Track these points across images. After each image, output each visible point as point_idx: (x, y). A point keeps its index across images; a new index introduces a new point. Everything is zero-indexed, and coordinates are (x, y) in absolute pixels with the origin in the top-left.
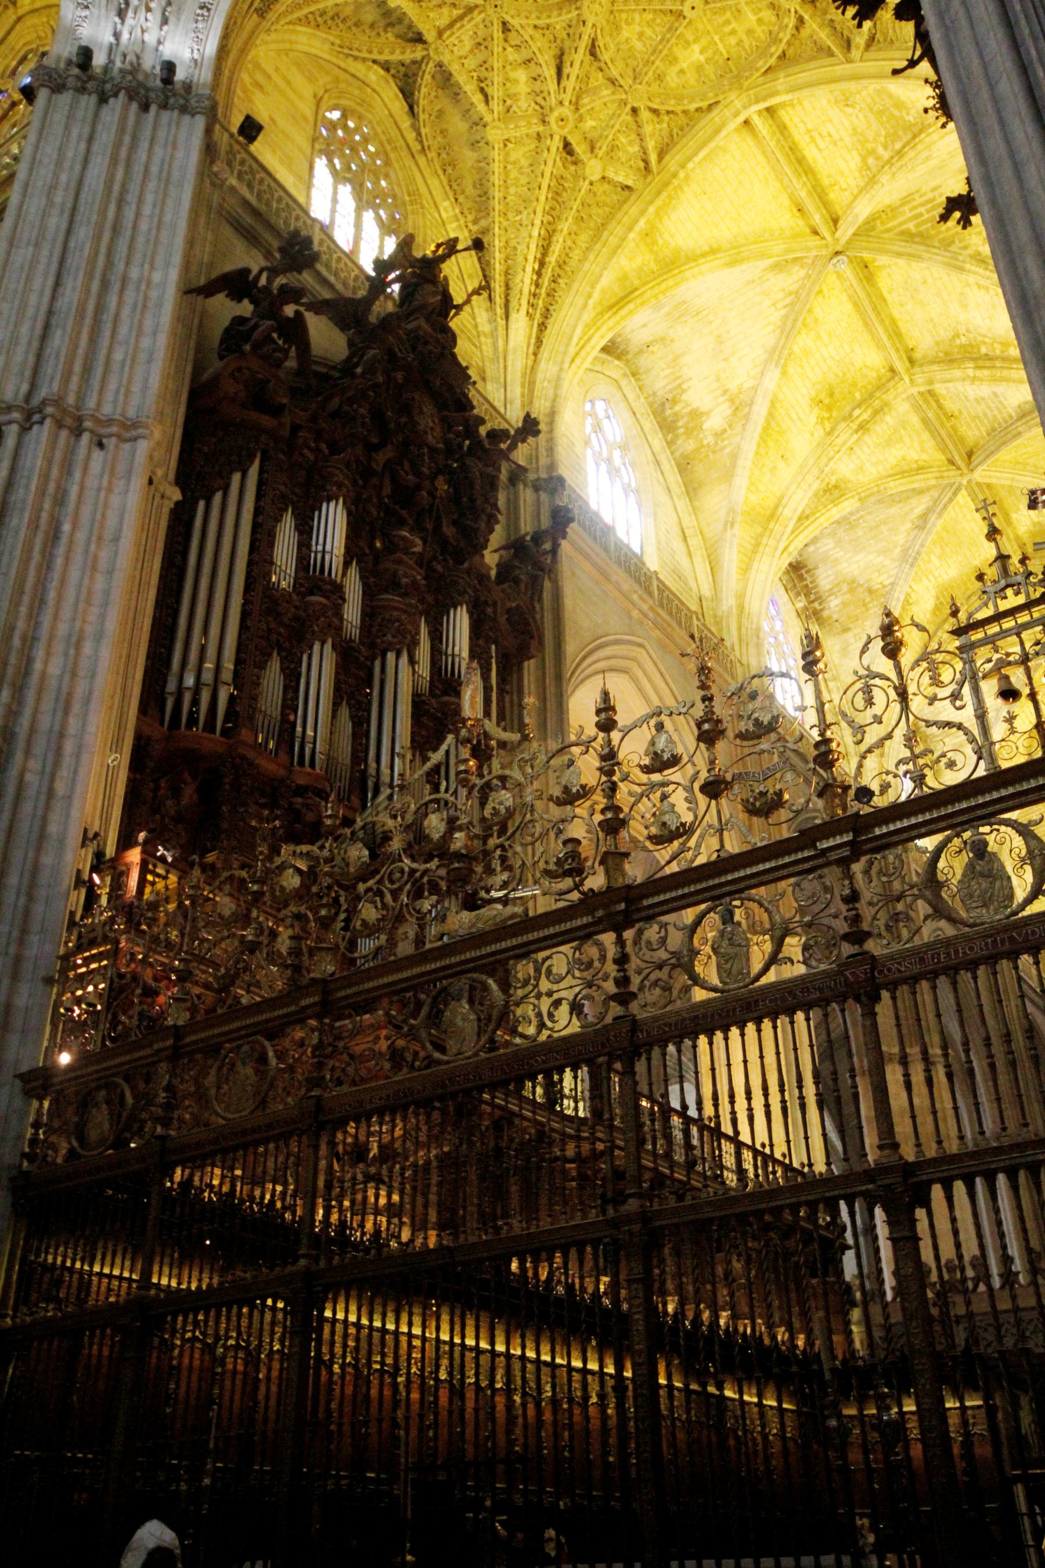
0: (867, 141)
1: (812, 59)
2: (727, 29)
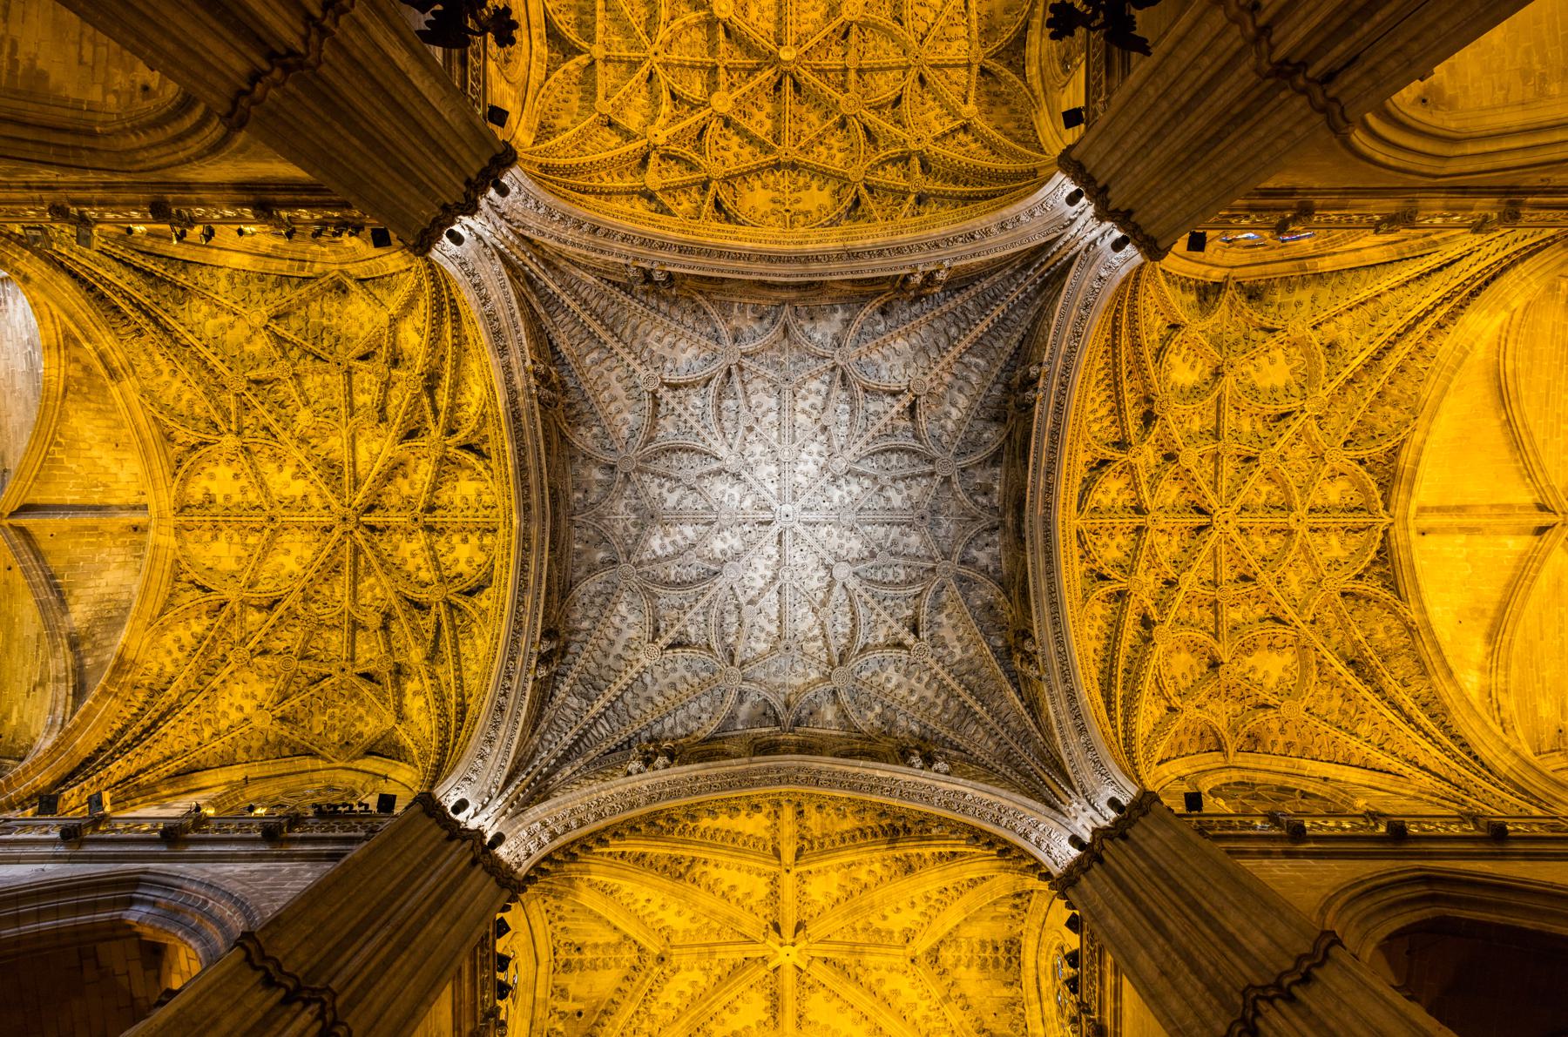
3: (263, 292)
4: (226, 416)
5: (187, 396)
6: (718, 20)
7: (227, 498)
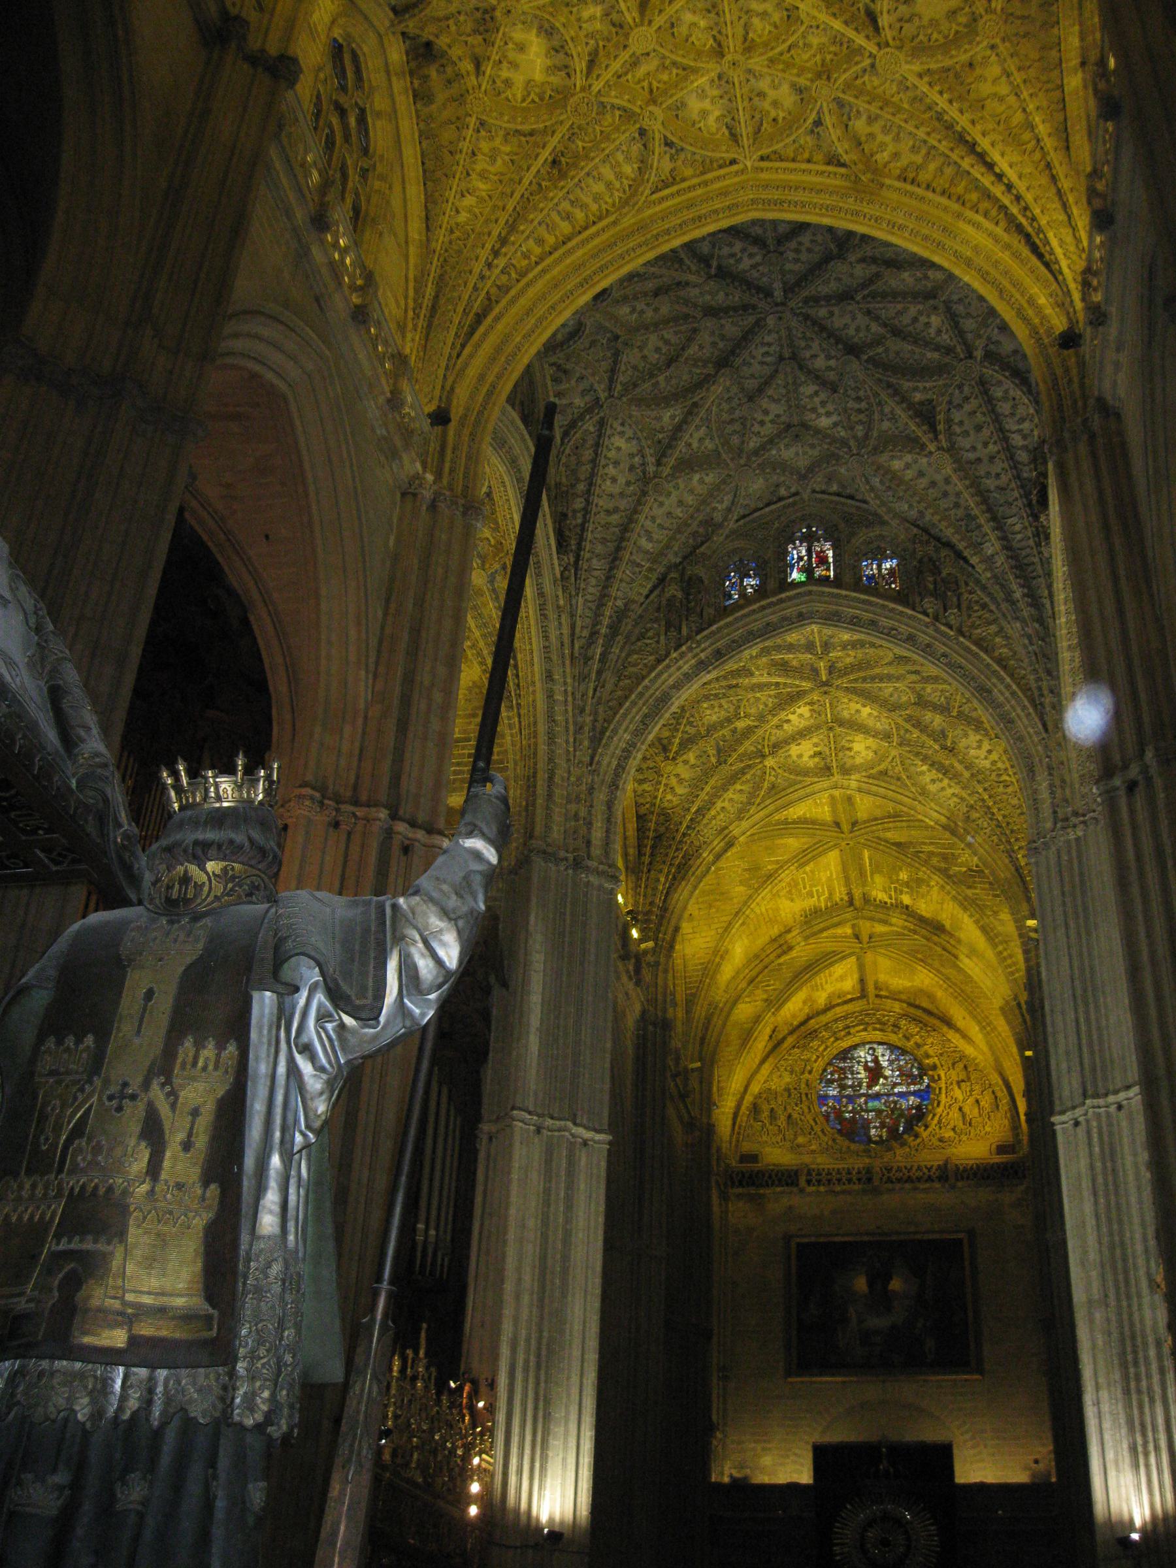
4: (749, 766)
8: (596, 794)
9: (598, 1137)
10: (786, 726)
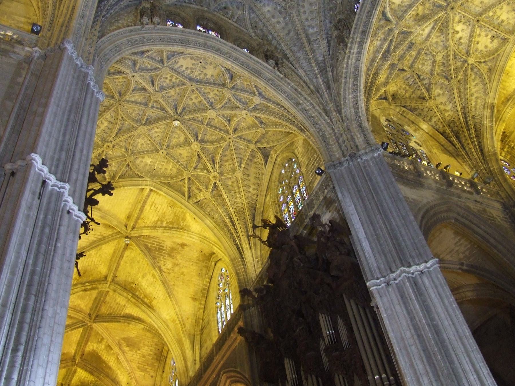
0: (164, 218)
1: (176, 191)
2: (161, 163)
3: (422, 110)
4: (466, 70)
5: (473, 84)
6: (199, 142)
7: (487, 35)
8: (351, 128)
9: (429, 264)
10: (462, 41)
